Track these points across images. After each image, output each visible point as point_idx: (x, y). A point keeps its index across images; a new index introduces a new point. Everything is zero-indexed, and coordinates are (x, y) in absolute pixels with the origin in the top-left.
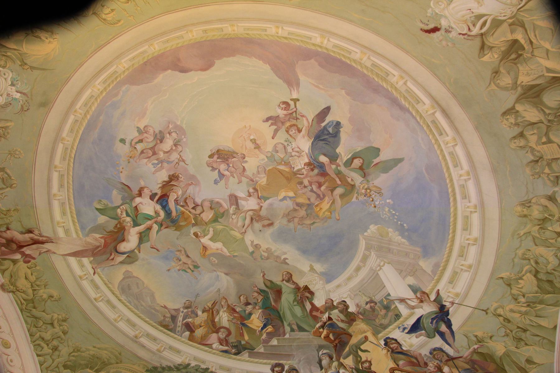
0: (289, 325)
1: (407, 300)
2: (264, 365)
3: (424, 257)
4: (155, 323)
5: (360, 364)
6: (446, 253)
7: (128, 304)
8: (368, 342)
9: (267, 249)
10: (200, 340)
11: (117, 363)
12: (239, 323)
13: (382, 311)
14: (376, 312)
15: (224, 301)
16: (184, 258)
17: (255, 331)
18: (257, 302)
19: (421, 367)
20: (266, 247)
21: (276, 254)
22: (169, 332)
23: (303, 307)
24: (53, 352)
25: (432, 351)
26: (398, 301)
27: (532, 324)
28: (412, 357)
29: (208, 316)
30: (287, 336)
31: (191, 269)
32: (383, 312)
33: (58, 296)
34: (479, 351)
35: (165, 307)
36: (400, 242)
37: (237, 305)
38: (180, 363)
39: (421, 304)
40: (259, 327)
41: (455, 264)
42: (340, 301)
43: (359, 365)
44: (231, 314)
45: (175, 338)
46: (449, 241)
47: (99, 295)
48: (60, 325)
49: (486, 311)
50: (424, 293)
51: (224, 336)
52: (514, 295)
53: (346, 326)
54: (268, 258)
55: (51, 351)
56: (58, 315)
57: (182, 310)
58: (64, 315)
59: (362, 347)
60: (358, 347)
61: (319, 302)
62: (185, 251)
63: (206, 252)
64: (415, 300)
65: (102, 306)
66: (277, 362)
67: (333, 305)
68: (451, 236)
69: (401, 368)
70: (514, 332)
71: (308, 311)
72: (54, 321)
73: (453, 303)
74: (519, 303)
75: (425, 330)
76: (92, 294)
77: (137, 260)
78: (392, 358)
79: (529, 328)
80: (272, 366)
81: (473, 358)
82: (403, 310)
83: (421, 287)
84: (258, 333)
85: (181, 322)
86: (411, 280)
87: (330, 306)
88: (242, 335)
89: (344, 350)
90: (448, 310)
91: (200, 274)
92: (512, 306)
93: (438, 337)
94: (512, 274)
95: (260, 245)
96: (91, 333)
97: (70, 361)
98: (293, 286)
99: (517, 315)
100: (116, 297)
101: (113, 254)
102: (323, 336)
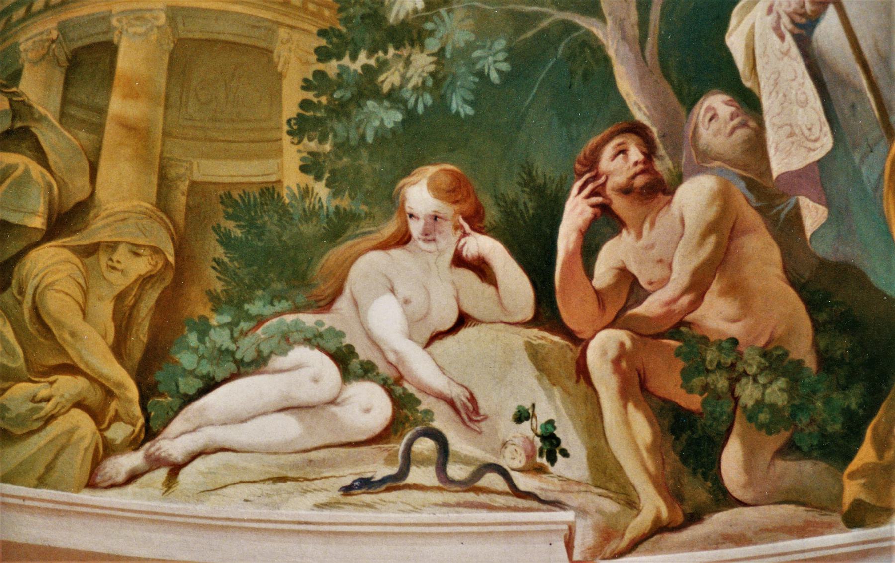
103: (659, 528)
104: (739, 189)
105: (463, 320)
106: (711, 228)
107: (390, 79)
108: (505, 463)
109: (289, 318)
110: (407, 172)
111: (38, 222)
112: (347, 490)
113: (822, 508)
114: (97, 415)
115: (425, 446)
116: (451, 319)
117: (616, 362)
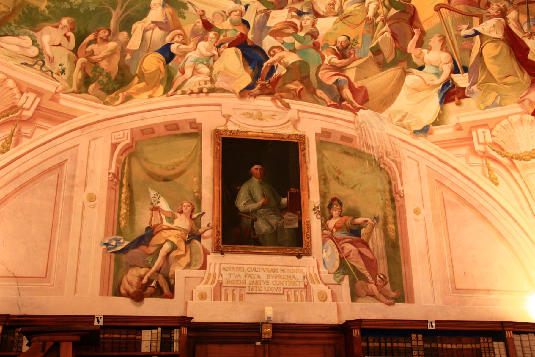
19: (479, 6)
69: (451, 6)
103: (74, 92)
104: (119, 48)
105: (60, 45)
106: (112, 51)
108: (53, 71)
109: (28, 31)
110: (65, 16)
112: (22, 64)
113: (101, 100)
115: (41, 62)
116: (58, 44)
117: (82, 64)
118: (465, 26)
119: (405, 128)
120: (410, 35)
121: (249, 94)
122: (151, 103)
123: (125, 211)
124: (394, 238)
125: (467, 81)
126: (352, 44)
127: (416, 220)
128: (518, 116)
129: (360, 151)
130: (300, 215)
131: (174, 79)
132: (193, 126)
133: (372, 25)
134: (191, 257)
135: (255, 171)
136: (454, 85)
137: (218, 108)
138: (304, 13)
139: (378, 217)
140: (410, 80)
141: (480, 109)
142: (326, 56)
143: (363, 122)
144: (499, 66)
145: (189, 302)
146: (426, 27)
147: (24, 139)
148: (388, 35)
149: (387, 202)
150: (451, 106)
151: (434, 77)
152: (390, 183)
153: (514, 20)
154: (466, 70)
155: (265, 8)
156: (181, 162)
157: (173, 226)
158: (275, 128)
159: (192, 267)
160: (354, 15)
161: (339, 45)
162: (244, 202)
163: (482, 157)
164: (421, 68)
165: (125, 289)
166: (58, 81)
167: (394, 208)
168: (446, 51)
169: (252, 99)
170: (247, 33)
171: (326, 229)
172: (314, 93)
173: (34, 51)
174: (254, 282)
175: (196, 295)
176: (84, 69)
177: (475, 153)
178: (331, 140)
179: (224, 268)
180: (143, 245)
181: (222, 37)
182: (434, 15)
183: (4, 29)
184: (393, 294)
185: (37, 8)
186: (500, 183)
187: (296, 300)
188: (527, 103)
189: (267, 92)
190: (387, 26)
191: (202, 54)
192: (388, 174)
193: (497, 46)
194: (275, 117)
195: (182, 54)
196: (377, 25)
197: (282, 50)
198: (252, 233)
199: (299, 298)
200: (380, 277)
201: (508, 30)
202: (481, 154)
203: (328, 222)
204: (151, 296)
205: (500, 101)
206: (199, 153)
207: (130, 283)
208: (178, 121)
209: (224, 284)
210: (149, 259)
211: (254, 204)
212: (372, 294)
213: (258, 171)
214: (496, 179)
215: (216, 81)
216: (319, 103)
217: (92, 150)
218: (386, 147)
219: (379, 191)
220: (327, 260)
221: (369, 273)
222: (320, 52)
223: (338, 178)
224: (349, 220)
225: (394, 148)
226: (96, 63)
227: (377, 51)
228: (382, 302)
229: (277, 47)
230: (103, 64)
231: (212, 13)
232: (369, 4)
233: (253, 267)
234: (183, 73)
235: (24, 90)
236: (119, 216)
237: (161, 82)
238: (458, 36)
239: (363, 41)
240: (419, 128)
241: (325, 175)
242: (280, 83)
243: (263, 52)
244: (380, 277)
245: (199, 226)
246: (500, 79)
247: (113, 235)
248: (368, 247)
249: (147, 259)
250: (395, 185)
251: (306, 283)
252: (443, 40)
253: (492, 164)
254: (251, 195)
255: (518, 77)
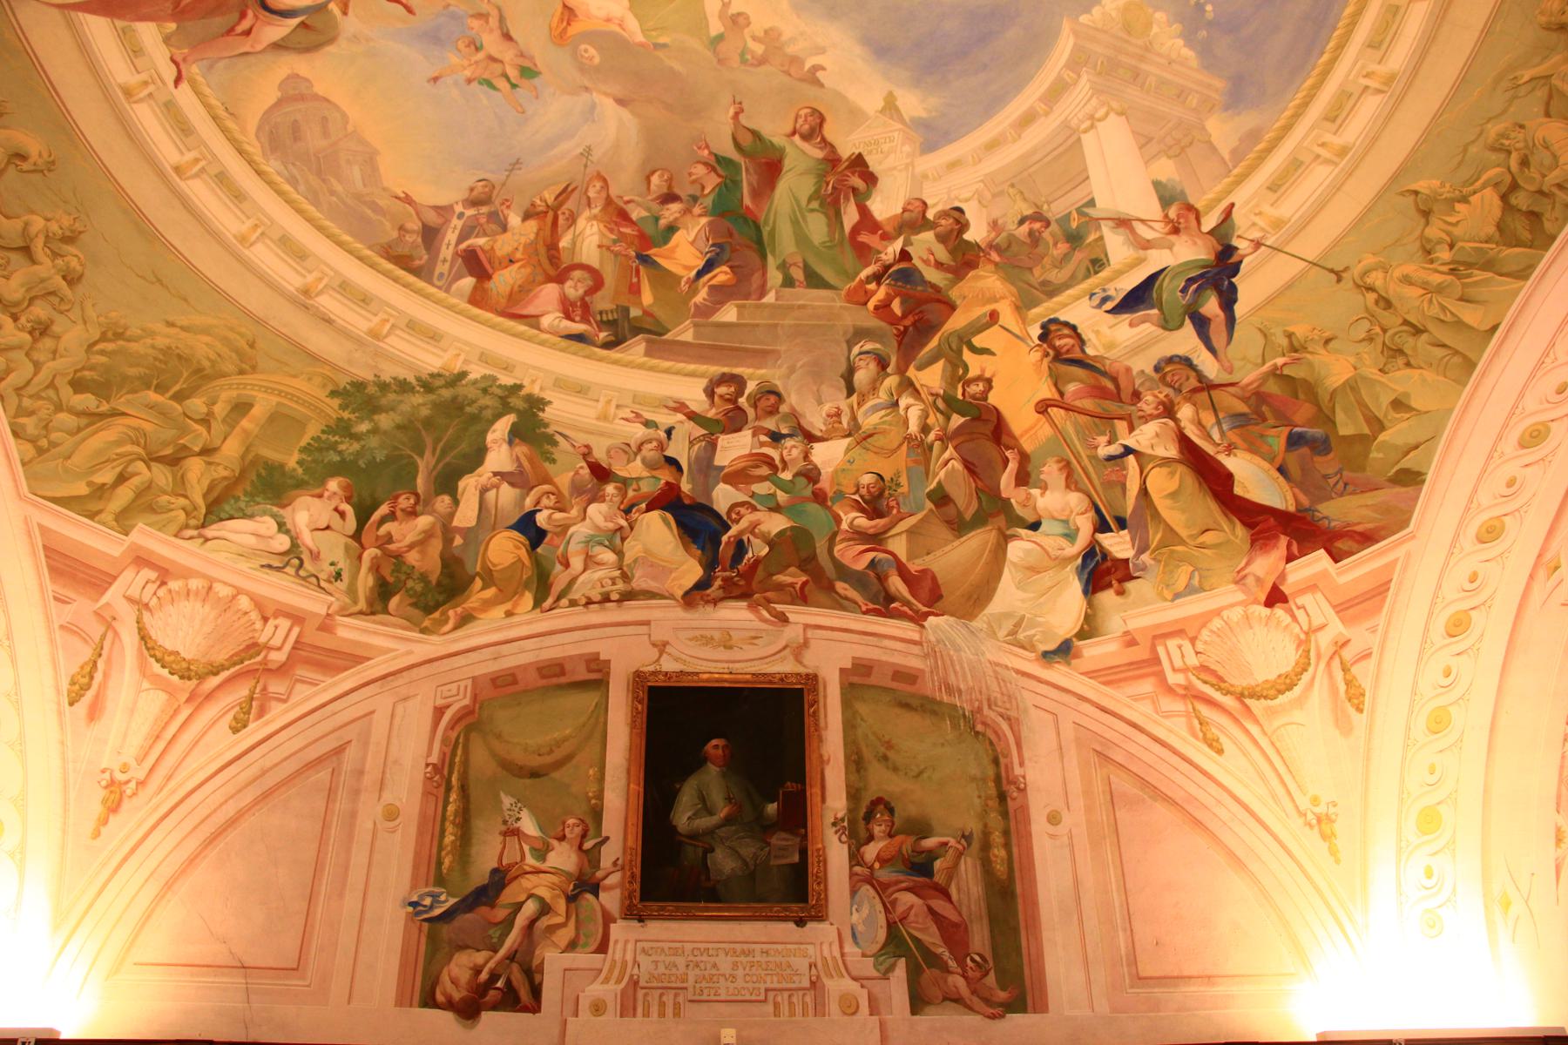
0: (784, 267)
1: (1137, 225)
2: (687, 379)
3: (1226, 108)
4: (370, 248)
5: (960, 386)
6: (1291, 104)
7: (287, 187)
8: (996, 327)
9: (766, 32)
10: (503, 301)
11: (242, 372)
12: (633, 254)
13: (1059, 245)
14: (1040, 249)
15: (598, 185)
16: (492, 43)
17: (677, 279)
18: (698, 194)
20: (767, 26)
21: (790, 50)
22: (411, 278)
23: (835, 217)
24: (35, 340)
25: (1163, 364)
26: (1110, 223)
27: (1442, 317)
28: (1104, 374)
29: (539, 230)
30: (770, 298)
31: (508, 79)
32: (1063, 247)
33: (45, 155)
34: (1286, 371)
35: (408, 200)
36: (1174, 56)
37: (636, 198)
38: (436, 371)
39: (1173, 238)
40: (688, 268)
41: (1304, 138)
42: (948, 207)
43: (956, 389)
44: (613, 226)
45: (427, 296)
46: (1317, 71)
47: (189, 156)
48: (56, 255)
49: (1339, 276)
50: (1190, 208)
51: (581, 292)
52: (1429, 240)
53: (946, 279)
54: (762, 61)
55: (28, 337)
56: (48, 220)
57: (459, 209)
58: (66, 221)
59: (978, 341)
60: (964, 339)
61: (884, 206)
62: (502, 19)
63: (569, 24)
64: (1157, 226)
65: (200, 191)
66: (726, 370)
67: (924, 216)
68: (1325, 57)
70: (1389, 333)
71: (848, 227)
72: (32, 240)
73: (1258, 244)
74: (1432, 262)
75: (1161, 309)
76: (168, 151)
77: (331, 40)
78: (1050, 376)
79: (1431, 326)
80: (711, 380)
81: (1264, 389)
82: (1117, 247)
83: (1188, 191)
84: (684, 286)
85: (451, 248)
86: (1166, 170)
87: (914, 220)
88: (635, 290)
89: (923, 345)
90: (1241, 262)
91: (537, 97)
92: (1410, 269)
93: (1189, 328)
94: (1448, 185)
95: (747, 18)
96: (159, 280)
97: (91, 369)
98: (819, 154)
99: (1413, 293)
100: (251, 162)
101: (250, 14)
102: (871, 305)
103: (361, 613)
104: (438, 526)
105: (328, 528)
106: (424, 532)
107: (342, 447)
110: (332, 476)
111: (197, 449)
112: (262, 566)
113: (415, 624)
114: (187, 514)
115: (296, 562)
116: (324, 526)
118: (1103, 439)
119: (1023, 647)
120: (1000, 465)
121: (702, 599)
122: (511, 626)
123: (453, 838)
124: (1004, 877)
125: (1129, 546)
126: (890, 488)
127: (1052, 836)
128: (1239, 610)
129: (933, 701)
130: (805, 837)
131: (551, 578)
132: (593, 666)
133: (920, 448)
134: (577, 928)
135: (712, 751)
136: (1105, 555)
137: (644, 629)
138: (784, 436)
139: (971, 833)
140: (1016, 549)
141: (1166, 600)
142: (842, 514)
143: (938, 642)
144: (1184, 511)
145: (570, 1019)
146: (1027, 445)
147: (274, 704)
148: (956, 465)
149: (990, 803)
150: (1107, 598)
151: (1063, 542)
152: (996, 762)
153: (1192, 422)
154: (1122, 523)
155: (704, 432)
156: (565, 739)
157: (543, 866)
158: (756, 663)
159: (579, 949)
160: (883, 432)
161: (864, 491)
162: (689, 814)
163: (1184, 697)
164: (1035, 526)
165: (444, 994)
166: (331, 594)
167: (1005, 814)
168: (1078, 490)
169: (709, 608)
170: (679, 481)
171: (858, 864)
172: (831, 588)
173: (283, 543)
174: (704, 977)
175: (584, 1004)
176: (377, 570)
177: (1170, 690)
178: (873, 680)
179: (643, 950)
180: (485, 904)
181: (631, 493)
182: (1038, 420)
183: (227, 507)
184: (1002, 995)
185: (282, 466)
186: (1225, 747)
187: (792, 1014)
188: (1250, 581)
189: (737, 592)
190: (950, 448)
191: (597, 528)
192: (991, 743)
193: (1172, 474)
194: (755, 641)
195: (559, 529)
196: (931, 447)
197: (754, 509)
198: (703, 877)
199: (799, 1009)
200: (973, 960)
201: (1184, 442)
202: (1182, 692)
203: (862, 850)
204: (495, 1007)
205: (1200, 581)
206: (602, 720)
207: (454, 982)
208: (564, 658)
209: (642, 983)
210: (495, 933)
211: (708, 819)
212: (956, 997)
213: (720, 752)
214: (1217, 740)
215: (633, 576)
216: (844, 608)
217: (397, 720)
218: (988, 688)
219: (973, 779)
220: (860, 928)
221: (950, 953)
222: (829, 508)
223: (885, 758)
224: (906, 844)
225: (1004, 689)
226: (398, 556)
227: (941, 498)
228: (978, 1013)
229: (742, 504)
230: (413, 558)
231: (604, 449)
232: (907, 408)
233: (702, 946)
234: (567, 565)
235: (268, 614)
236: (441, 848)
237: (526, 586)
238: (1093, 458)
239: (909, 478)
240: (1052, 646)
241: (859, 753)
242: (760, 573)
243: (717, 516)
244: (973, 960)
245: (596, 864)
246: (1191, 537)
247: (427, 885)
248: (948, 897)
249: (491, 932)
250: (1006, 766)
251: (814, 978)
252: (1067, 467)
253: (1205, 710)
254: (703, 799)
255: (1223, 531)
